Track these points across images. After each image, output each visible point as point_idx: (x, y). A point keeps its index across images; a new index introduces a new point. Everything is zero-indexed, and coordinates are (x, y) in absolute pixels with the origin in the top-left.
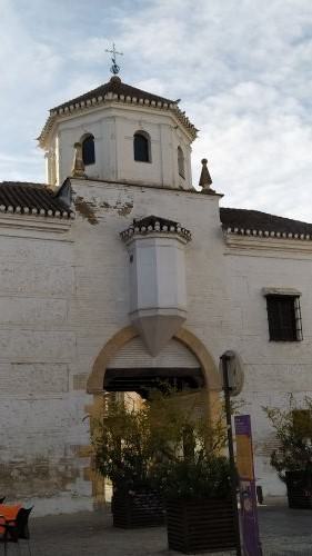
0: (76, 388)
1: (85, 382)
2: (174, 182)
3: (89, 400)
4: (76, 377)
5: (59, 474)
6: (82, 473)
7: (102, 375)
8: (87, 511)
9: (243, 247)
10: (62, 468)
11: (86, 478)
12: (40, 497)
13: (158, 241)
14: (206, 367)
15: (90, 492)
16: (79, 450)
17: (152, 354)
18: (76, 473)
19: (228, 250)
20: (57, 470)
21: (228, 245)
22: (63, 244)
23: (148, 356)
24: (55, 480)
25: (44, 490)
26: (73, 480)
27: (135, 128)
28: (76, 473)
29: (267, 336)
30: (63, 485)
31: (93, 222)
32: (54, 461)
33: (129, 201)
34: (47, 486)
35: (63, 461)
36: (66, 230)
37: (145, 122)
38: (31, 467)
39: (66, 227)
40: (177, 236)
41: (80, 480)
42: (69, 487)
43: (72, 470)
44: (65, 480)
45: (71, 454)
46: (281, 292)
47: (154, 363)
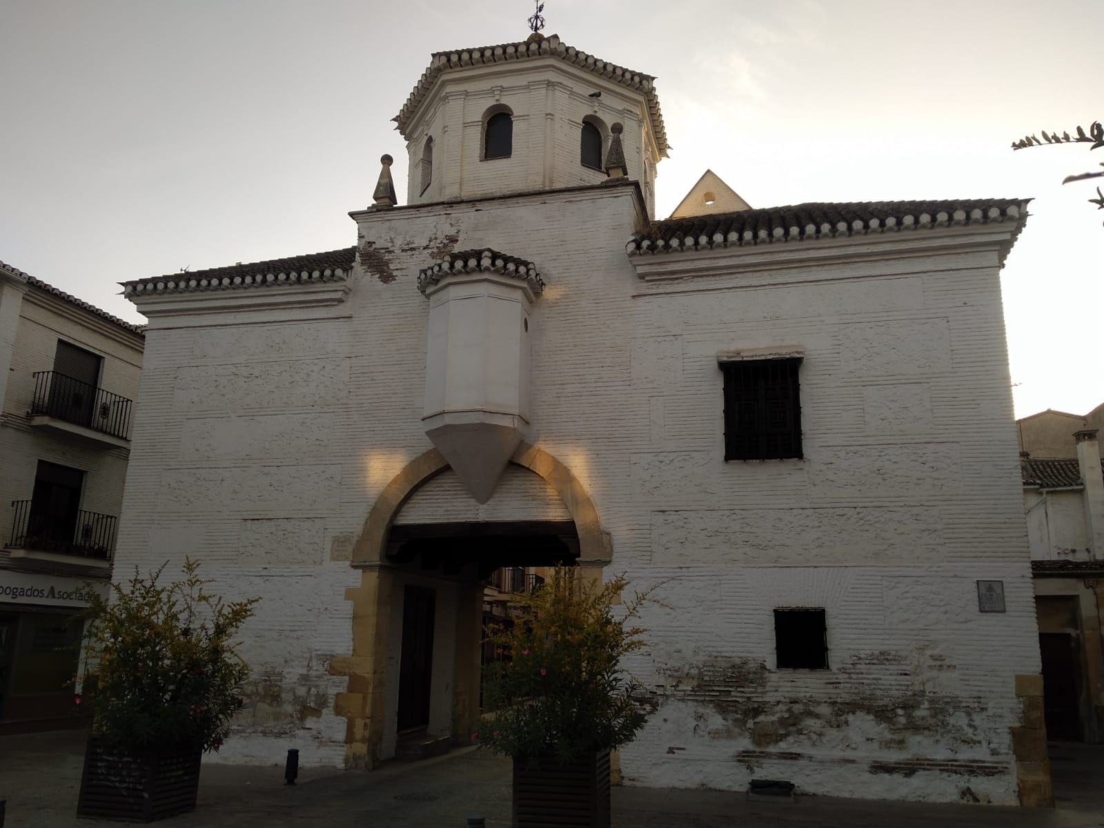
0: (334, 558)
1: (350, 549)
2: (551, 181)
3: (356, 578)
4: (336, 540)
5: (296, 699)
6: (331, 702)
7: (379, 534)
8: (335, 767)
9: (674, 276)
10: (302, 691)
11: (338, 711)
12: (264, 733)
13: (454, 292)
14: (579, 523)
15: (341, 736)
16: (334, 666)
17: (484, 496)
18: (322, 701)
19: (644, 288)
20: (293, 690)
21: (642, 277)
22: (336, 323)
23: (473, 502)
24: (289, 708)
25: (271, 723)
26: (316, 712)
27: (492, 102)
28: (322, 701)
29: (720, 451)
30: (302, 719)
31: (387, 277)
32: (292, 675)
33: (452, 232)
34: (277, 717)
35: (305, 678)
36: (340, 301)
37: (502, 89)
38: (256, 684)
39: (339, 295)
40: (486, 276)
41: (328, 713)
42: (310, 722)
43: (318, 695)
44: (307, 710)
45: (318, 668)
46: (747, 356)
47: (483, 513)
